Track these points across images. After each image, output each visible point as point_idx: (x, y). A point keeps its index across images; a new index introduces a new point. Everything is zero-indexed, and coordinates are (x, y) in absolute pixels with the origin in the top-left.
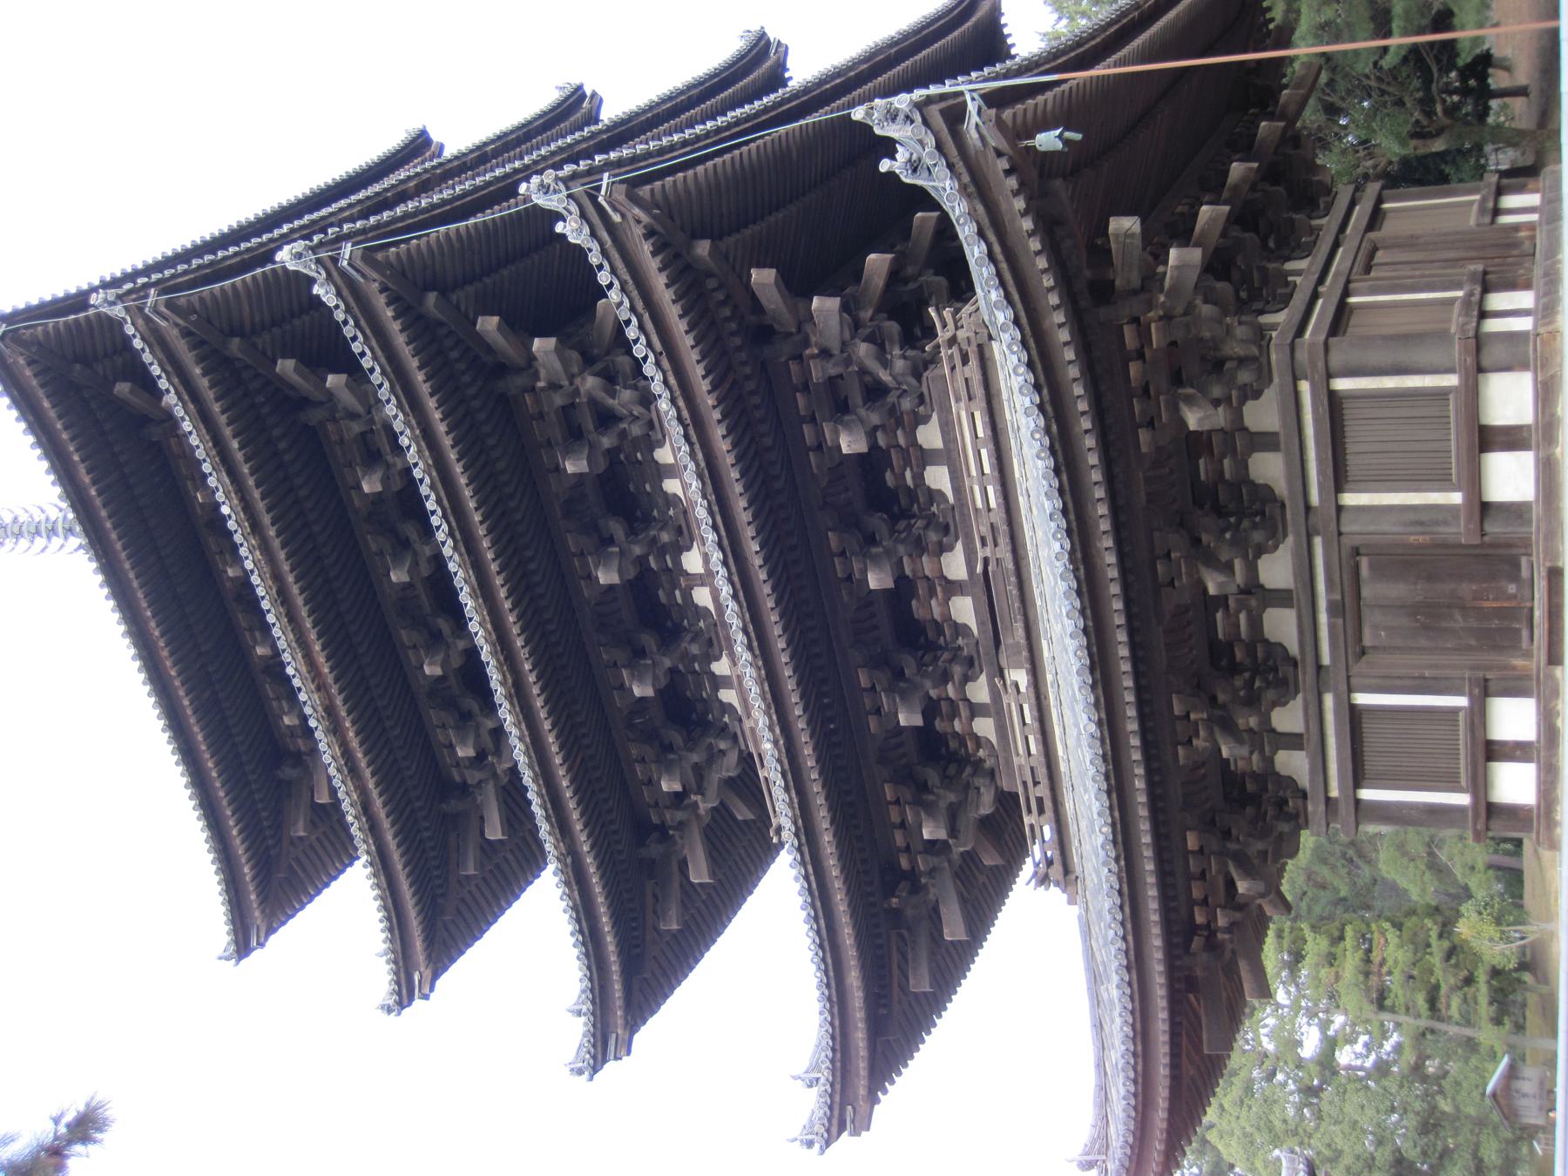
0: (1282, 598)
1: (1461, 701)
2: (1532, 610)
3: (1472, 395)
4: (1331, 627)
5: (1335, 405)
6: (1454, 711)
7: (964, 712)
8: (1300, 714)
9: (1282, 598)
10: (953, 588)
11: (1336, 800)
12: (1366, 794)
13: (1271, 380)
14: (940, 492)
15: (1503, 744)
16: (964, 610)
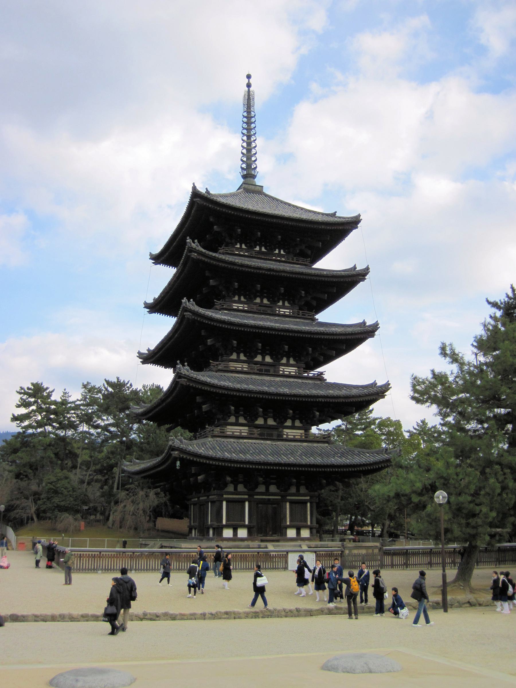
0: (267, 489)
1: (247, 523)
2: (267, 536)
3: (306, 527)
4: (265, 499)
5: (305, 503)
6: (244, 521)
7: (237, 415)
8: (242, 491)
9: (267, 489)
10: (266, 420)
11: (223, 496)
12: (224, 503)
13: (309, 492)
14: (286, 422)
15: (237, 531)
16: (260, 421)
